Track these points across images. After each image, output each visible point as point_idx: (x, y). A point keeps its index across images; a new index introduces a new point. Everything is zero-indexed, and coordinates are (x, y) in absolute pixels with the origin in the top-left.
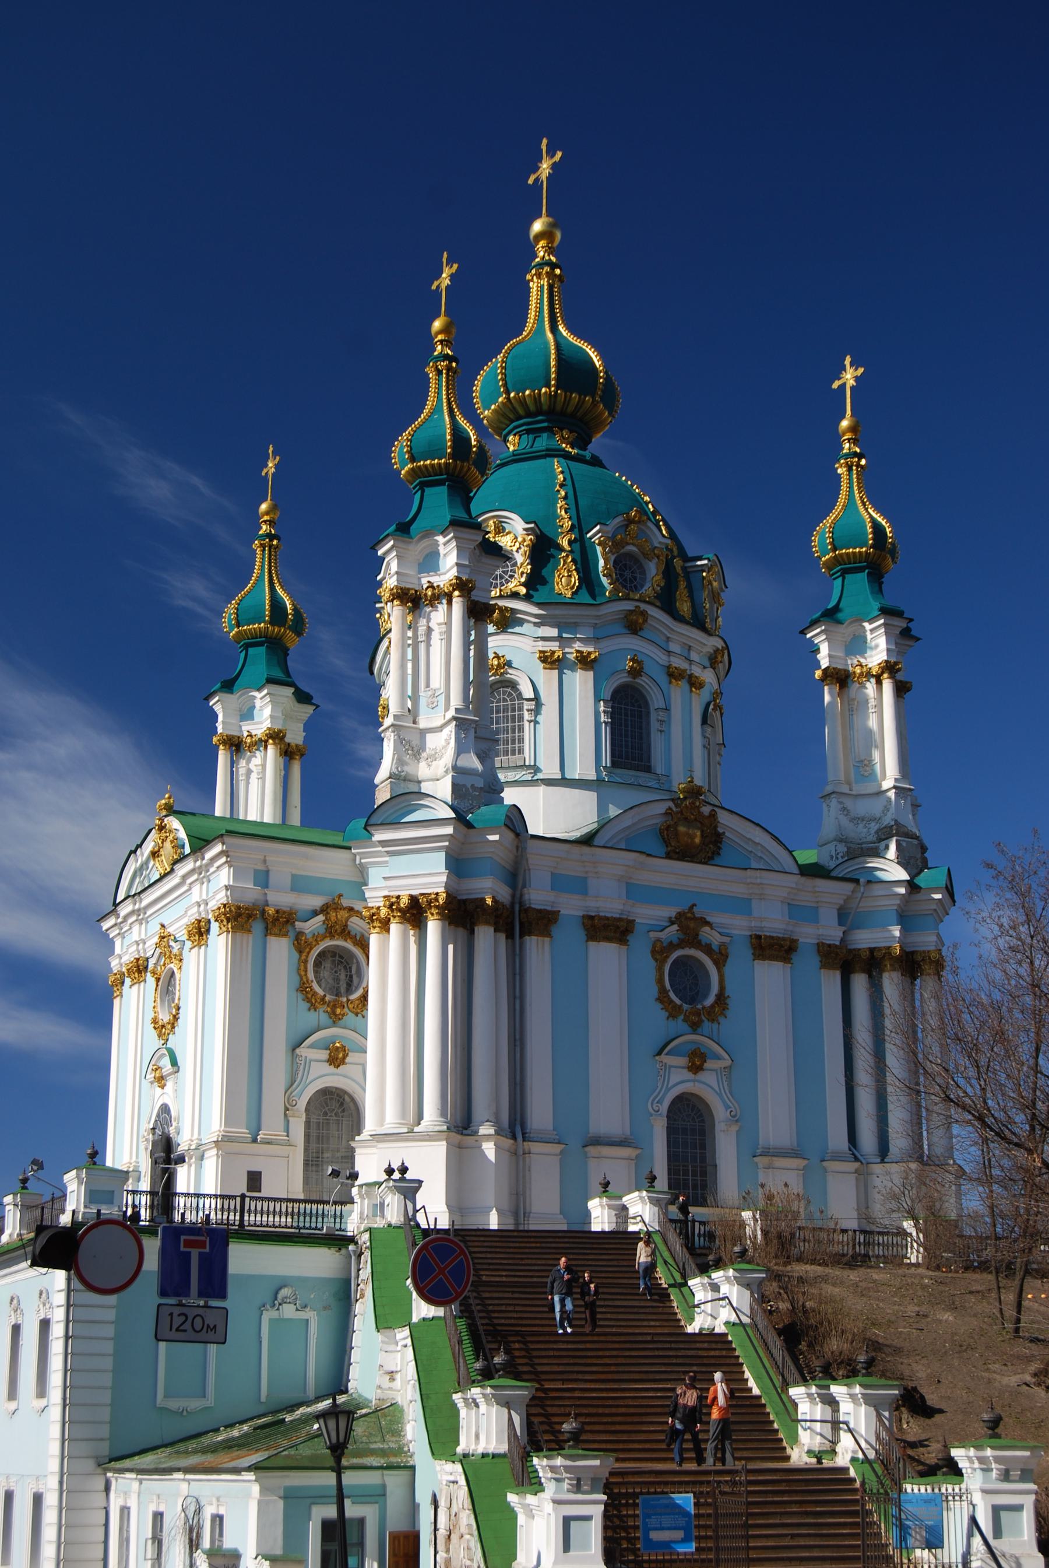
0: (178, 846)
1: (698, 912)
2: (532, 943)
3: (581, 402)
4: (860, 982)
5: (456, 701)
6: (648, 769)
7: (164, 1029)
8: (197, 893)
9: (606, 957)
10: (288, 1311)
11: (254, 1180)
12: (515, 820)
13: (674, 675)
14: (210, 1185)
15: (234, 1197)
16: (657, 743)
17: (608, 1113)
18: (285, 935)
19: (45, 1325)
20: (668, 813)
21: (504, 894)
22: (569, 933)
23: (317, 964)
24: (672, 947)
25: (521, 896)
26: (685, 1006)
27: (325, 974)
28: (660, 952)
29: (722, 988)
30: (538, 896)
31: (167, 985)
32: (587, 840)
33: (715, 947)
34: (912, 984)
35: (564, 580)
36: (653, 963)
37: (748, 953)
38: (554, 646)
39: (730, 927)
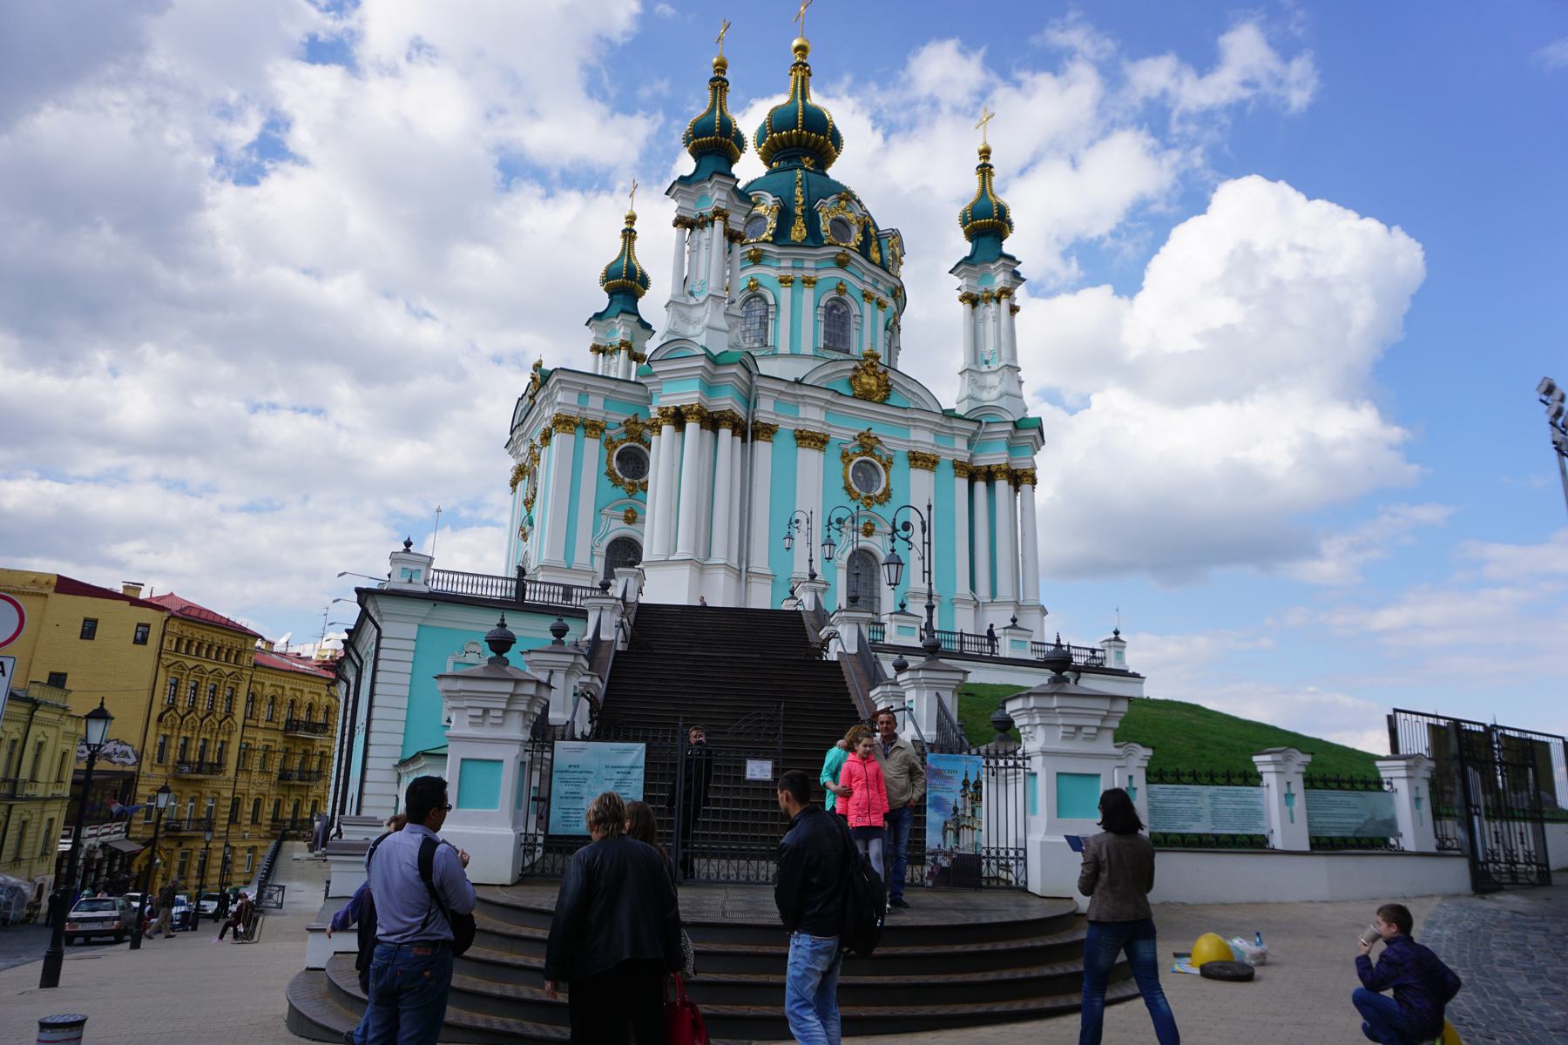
1: (873, 432)
3: (817, 140)
4: (980, 486)
5: (712, 284)
7: (529, 503)
16: (854, 336)
20: (855, 369)
21: (740, 412)
22: (784, 440)
23: (618, 458)
26: (863, 494)
28: (846, 457)
29: (888, 484)
32: (798, 382)
34: (1017, 490)
35: (798, 232)
37: (907, 464)
38: (789, 273)
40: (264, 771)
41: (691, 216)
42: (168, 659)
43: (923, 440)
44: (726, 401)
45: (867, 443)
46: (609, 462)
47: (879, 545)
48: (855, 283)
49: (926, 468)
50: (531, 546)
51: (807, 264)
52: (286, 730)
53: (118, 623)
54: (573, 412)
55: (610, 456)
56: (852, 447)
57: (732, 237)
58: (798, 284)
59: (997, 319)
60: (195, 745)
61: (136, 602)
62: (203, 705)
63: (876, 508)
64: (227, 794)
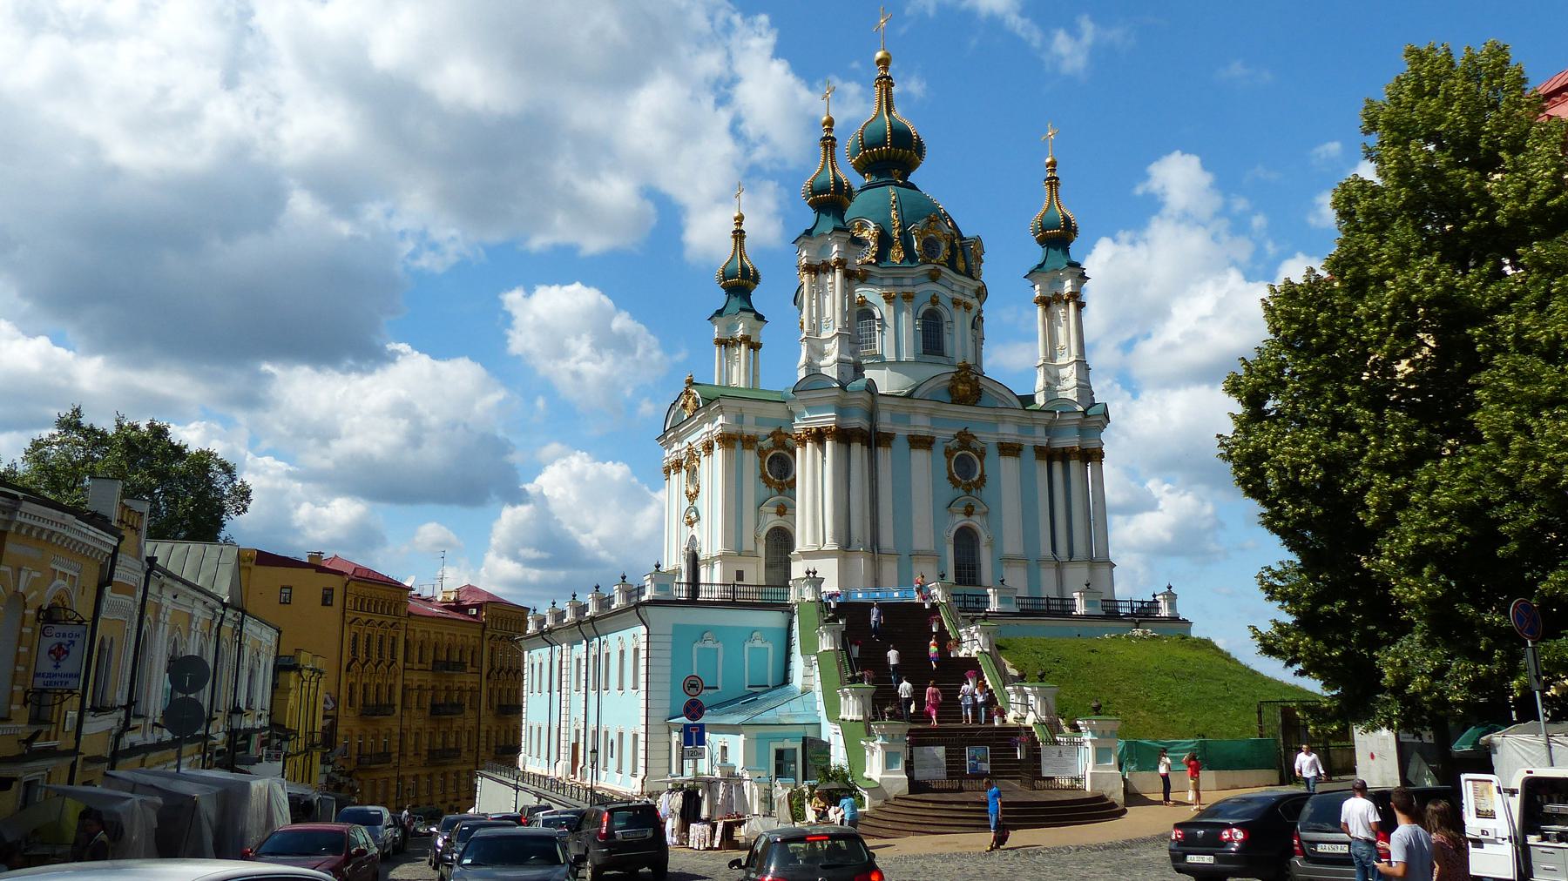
0: (696, 401)
2: (880, 450)
5: (838, 325)
6: (942, 355)
7: (692, 497)
8: (707, 428)
9: (920, 457)
10: (758, 643)
11: (740, 575)
12: (871, 387)
13: (956, 303)
14: (717, 579)
16: (947, 338)
17: (922, 539)
19: (636, 651)
20: (953, 379)
21: (865, 425)
22: (901, 444)
27: (774, 468)
28: (949, 453)
31: (693, 474)
32: (909, 396)
36: (944, 460)
40: (419, 707)
41: (818, 262)
42: (350, 616)
43: (1009, 432)
44: (857, 421)
45: (965, 439)
46: (762, 467)
47: (976, 522)
50: (700, 532)
51: (907, 281)
52: (433, 670)
53: (309, 587)
54: (734, 429)
55: (763, 462)
56: (954, 444)
58: (899, 300)
60: (372, 689)
61: (321, 569)
62: (375, 657)
64: (397, 730)
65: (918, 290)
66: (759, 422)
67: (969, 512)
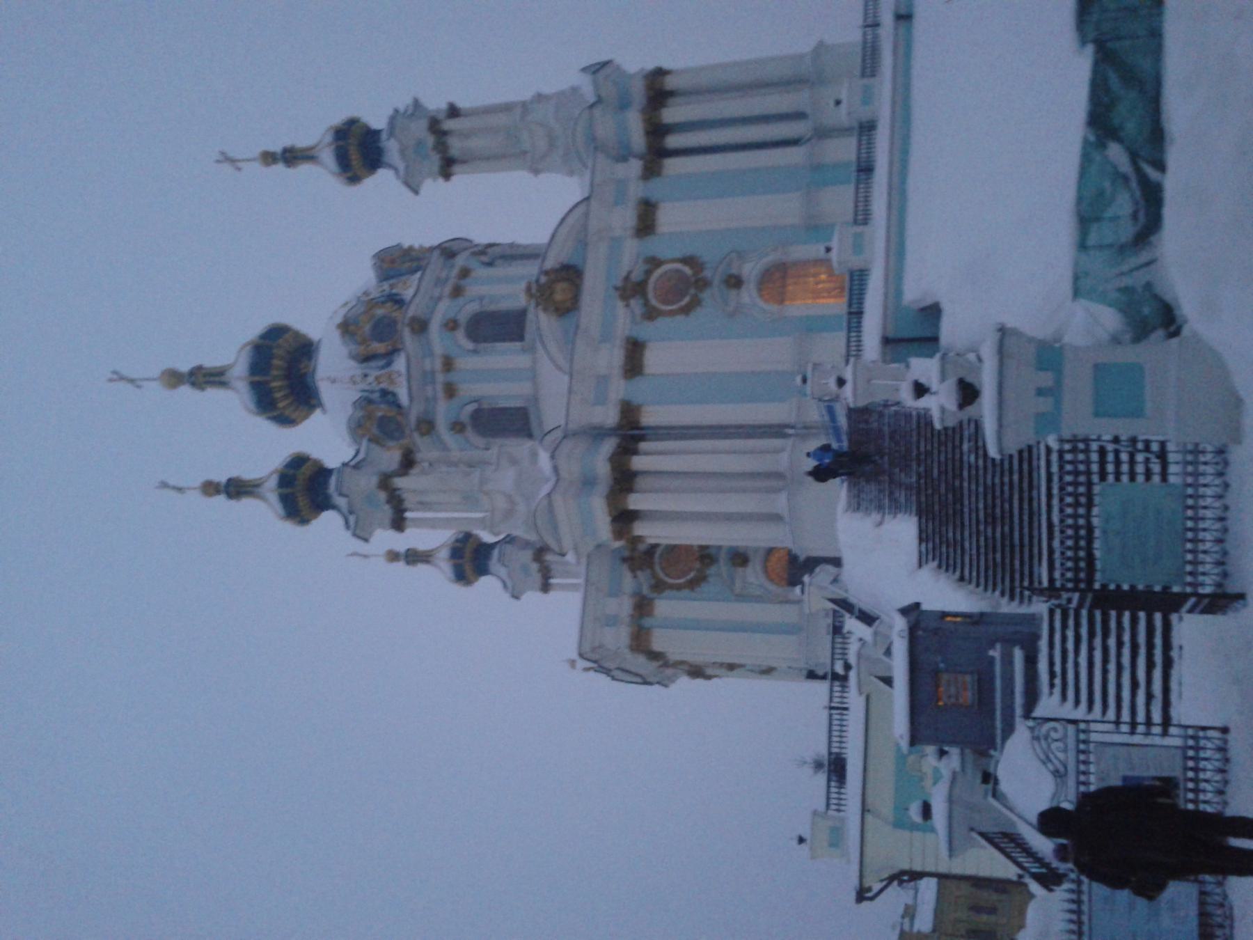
4: (673, 141)
7: (731, 667)
9: (653, 359)
15: (831, 715)
16: (505, 305)
18: (652, 600)
20: (545, 310)
21: (609, 446)
22: (638, 391)
24: (646, 303)
25: (611, 429)
26: (692, 291)
28: (651, 314)
30: (609, 416)
33: (646, 267)
34: (671, 94)
36: (660, 319)
39: (631, 253)
41: (387, 511)
45: (632, 289)
46: (679, 588)
47: (750, 270)
48: (444, 309)
49: (654, 213)
55: (672, 587)
57: (408, 463)
58: (453, 377)
59: (467, 135)
63: (707, 273)
65: (438, 350)
66: (615, 592)
67: (735, 282)
